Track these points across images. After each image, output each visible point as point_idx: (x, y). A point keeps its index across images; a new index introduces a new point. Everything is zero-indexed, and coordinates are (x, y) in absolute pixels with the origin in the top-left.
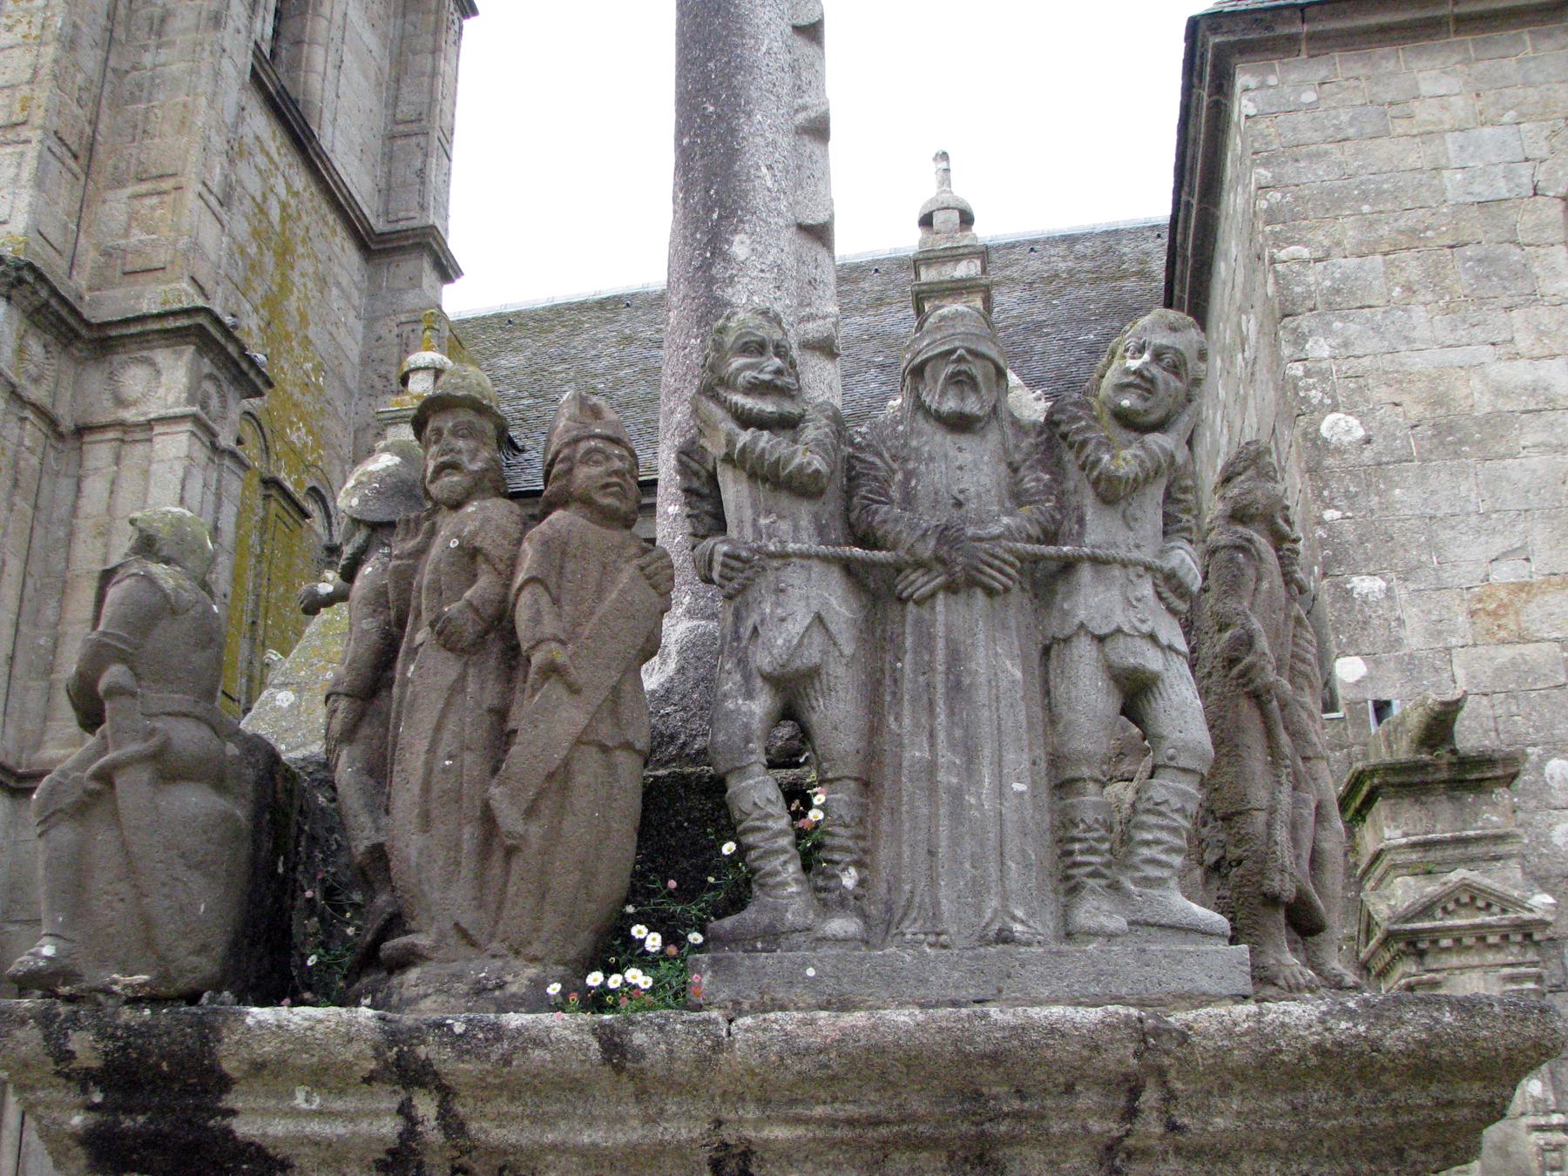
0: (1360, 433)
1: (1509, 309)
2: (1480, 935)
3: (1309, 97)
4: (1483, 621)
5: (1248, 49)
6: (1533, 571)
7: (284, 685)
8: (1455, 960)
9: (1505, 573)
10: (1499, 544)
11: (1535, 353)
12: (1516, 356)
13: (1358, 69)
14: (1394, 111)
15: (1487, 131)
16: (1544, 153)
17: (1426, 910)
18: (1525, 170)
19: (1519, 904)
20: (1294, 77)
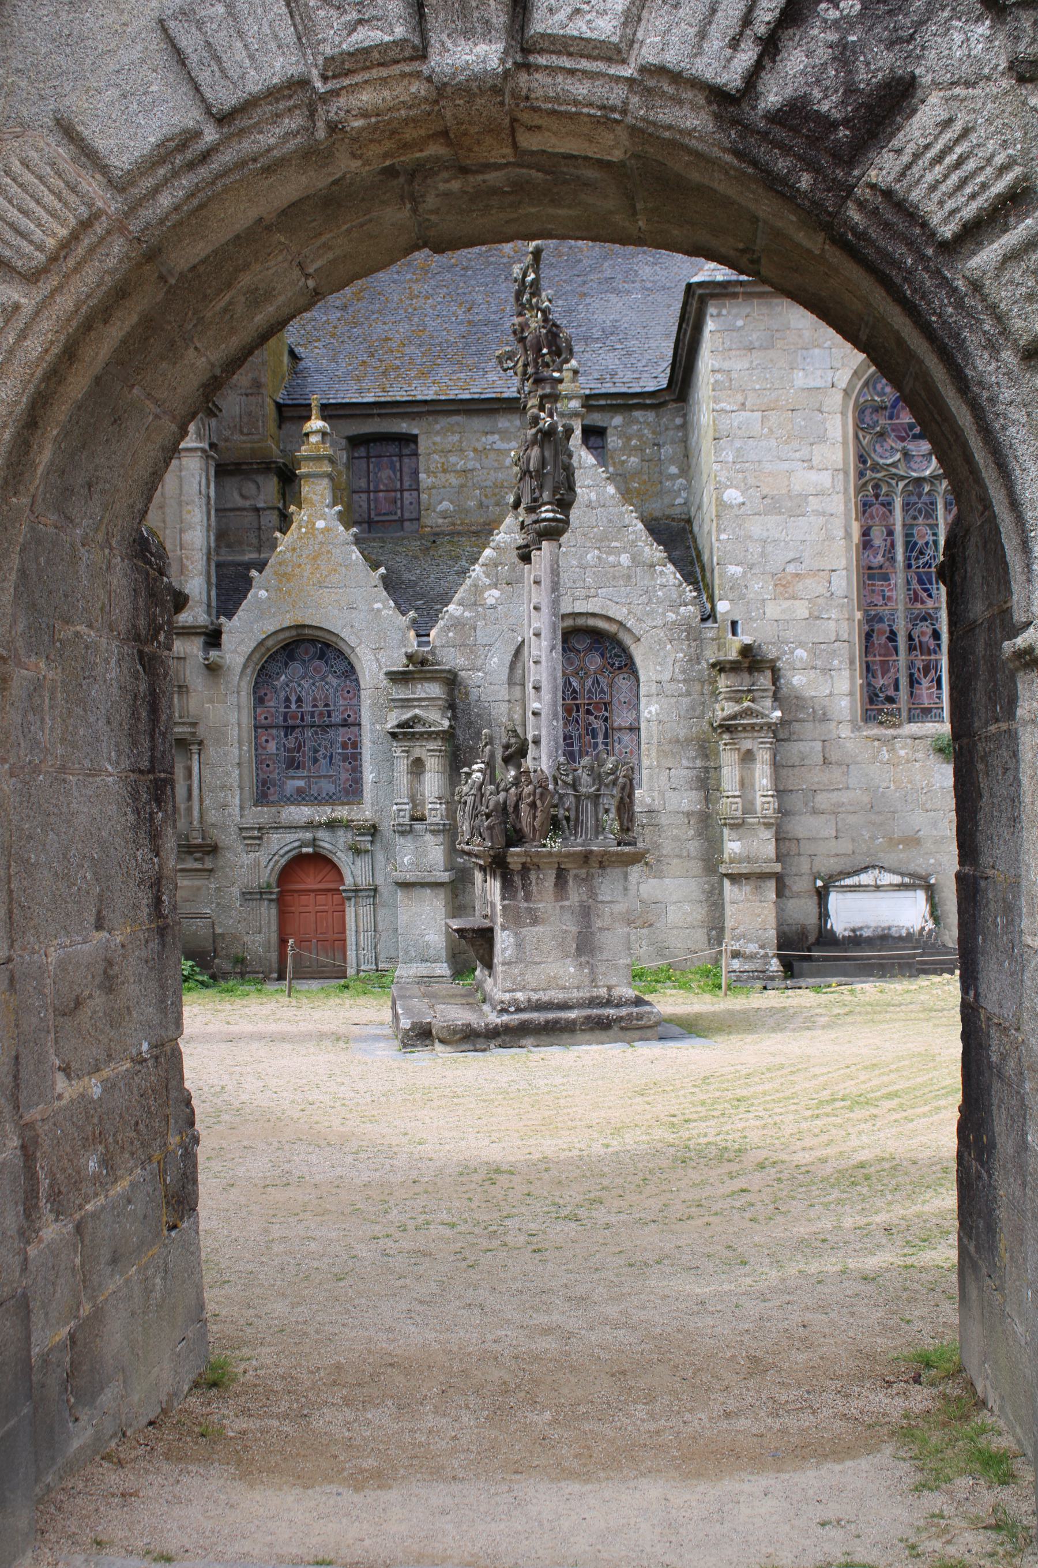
0: (741, 500)
1: (812, 444)
2: (753, 726)
3: (740, 323)
4: (780, 589)
5: (713, 296)
6: (802, 569)
7: (260, 588)
8: (743, 735)
9: (791, 569)
10: (791, 555)
12: (812, 468)
13: (764, 310)
14: (777, 335)
15: (817, 351)
16: (839, 365)
17: (734, 717)
18: (830, 373)
19: (767, 716)
20: (734, 311)
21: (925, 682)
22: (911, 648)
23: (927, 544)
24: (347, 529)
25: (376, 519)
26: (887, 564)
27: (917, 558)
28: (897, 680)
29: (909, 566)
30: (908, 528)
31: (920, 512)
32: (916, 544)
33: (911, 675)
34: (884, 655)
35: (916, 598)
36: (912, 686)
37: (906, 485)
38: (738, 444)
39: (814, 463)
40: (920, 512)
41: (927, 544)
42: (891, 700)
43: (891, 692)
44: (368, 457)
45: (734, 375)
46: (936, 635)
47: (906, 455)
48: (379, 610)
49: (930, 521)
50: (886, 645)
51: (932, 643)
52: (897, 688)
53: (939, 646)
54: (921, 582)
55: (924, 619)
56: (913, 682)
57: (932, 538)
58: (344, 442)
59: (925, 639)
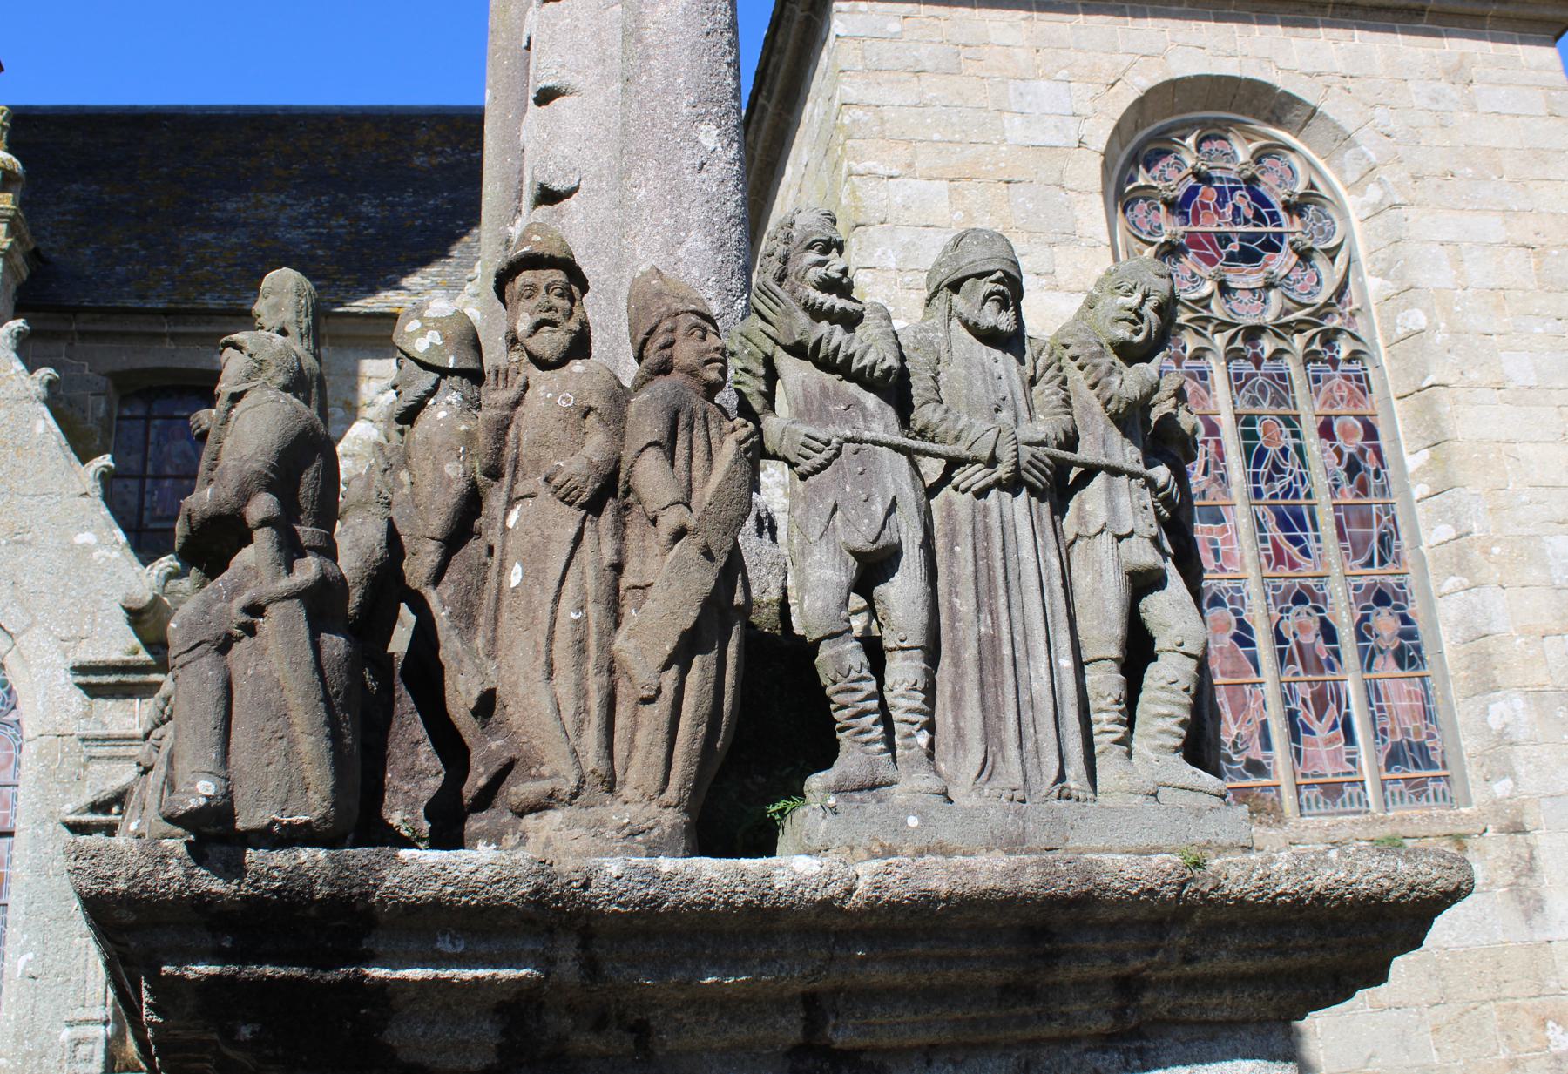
1: (1052, 244)
11: (1072, 287)
14: (965, 52)
15: (1043, 84)
16: (1088, 111)
18: (1072, 123)
21: (1321, 729)
22: (1283, 658)
23: (1284, 451)
24: (31, 369)
25: (152, 526)
26: (1214, 488)
27: (1270, 479)
28: (1264, 725)
29: (1258, 493)
30: (1246, 423)
31: (1263, 391)
32: (1262, 452)
33: (1292, 715)
34: (1233, 674)
35: (1279, 557)
36: (1295, 737)
37: (1232, 339)
38: (905, 236)
39: (1062, 279)
40: (1263, 391)
41: (1284, 451)
42: (1256, 768)
43: (1256, 752)
44: (148, 418)
45: (889, 113)
46: (1328, 632)
47: (1224, 289)
48: (87, 549)
49: (1283, 410)
50: (1233, 652)
51: (1322, 649)
52: (1267, 744)
53: (1336, 653)
54: (1283, 524)
55: (1299, 599)
56: (1296, 730)
57: (1291, 441)
58: (104, 382)
59: (1307, 639)
